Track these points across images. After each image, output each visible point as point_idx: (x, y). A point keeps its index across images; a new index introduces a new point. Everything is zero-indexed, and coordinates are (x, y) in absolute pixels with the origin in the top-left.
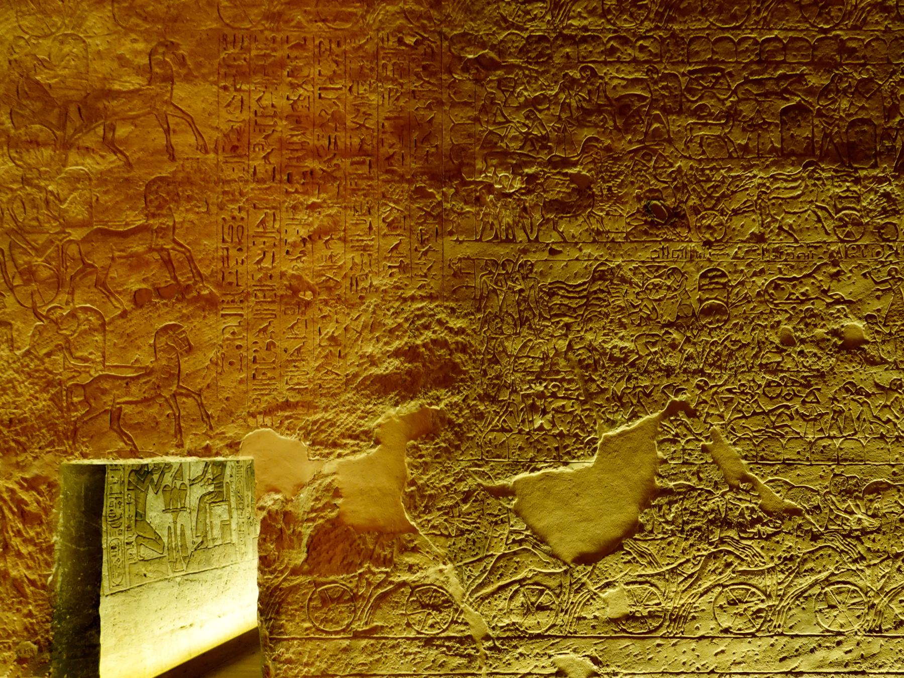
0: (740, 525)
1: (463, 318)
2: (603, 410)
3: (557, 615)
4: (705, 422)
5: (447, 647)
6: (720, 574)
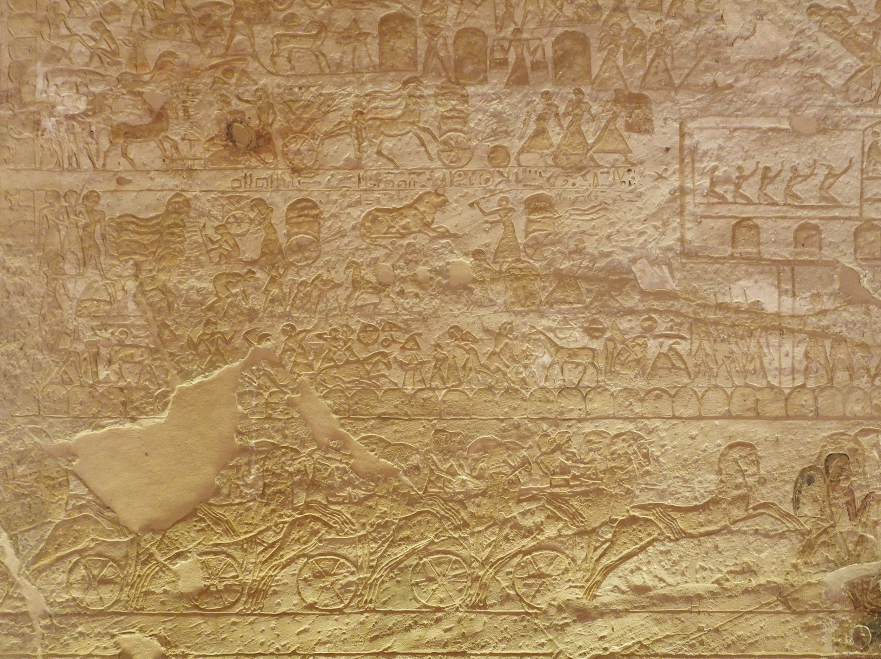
0: (330, 487)
1: (21, 256)
2: (176, 359)
3: (121, 590)
4: (292, 372)
6: (305, 543)
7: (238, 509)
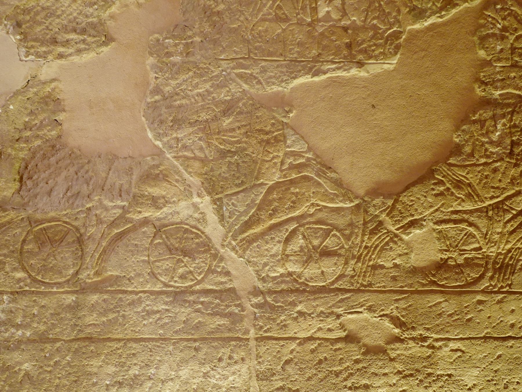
3: (346, 263)
5: (202, 303)
7: (483, 170)
